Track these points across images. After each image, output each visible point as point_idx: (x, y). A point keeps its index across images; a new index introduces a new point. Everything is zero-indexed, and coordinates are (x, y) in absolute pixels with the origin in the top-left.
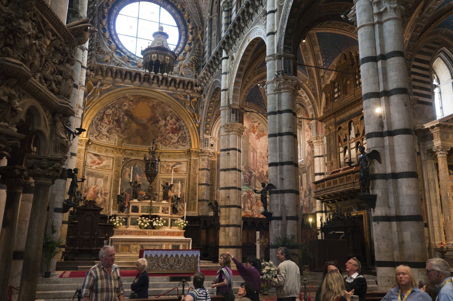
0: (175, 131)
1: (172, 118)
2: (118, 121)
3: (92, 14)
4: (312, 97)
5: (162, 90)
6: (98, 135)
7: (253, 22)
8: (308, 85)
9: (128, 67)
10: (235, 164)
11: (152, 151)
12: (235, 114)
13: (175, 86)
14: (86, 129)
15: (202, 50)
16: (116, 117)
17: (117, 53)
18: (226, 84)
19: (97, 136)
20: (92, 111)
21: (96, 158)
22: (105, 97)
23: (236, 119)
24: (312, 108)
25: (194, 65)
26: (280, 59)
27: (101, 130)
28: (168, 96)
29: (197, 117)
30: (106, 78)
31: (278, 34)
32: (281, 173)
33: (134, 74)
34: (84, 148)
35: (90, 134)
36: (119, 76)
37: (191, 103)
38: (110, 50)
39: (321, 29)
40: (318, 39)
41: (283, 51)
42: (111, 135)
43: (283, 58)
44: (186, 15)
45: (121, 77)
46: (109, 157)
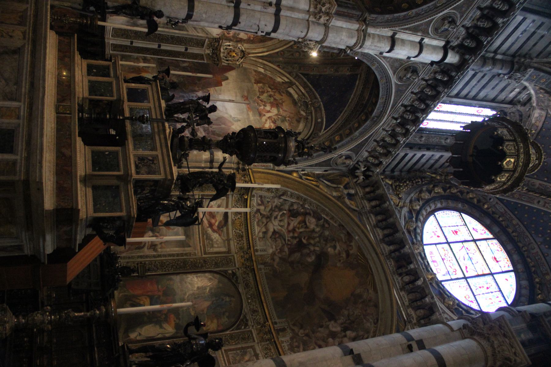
2: (300, 246)
16: (307, 240)
17: (410, 212)
19: (261, 214)
21: (220, 218)
22: (335, 203)
27: (273, 218)
30: (365, 201)
38: (408, 201)
42: (270, 240)
46: (229, 245)
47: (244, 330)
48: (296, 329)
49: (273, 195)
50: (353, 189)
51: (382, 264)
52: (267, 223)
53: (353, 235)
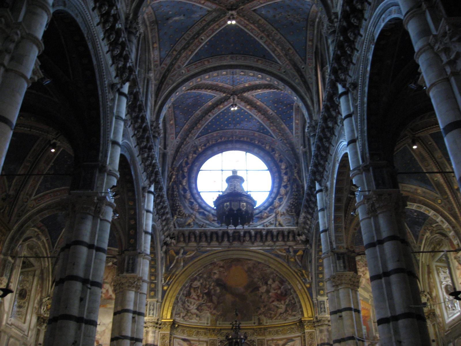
0: (280, 297)
1: (274, 281)
2: (209, 294)
3: (152, 172)
4: (451, 220)
5: (257, 247)
6: (186, 315)
7: (337, 137)
8: (441, 205)
9: (214, 227)
10: (351, 330)
11: (236, 326)
12: (341, 261)
13: (272, 239)
14: (15, 290)
15: (301, 190)
16: (206, 289)
17: (200, 213)
18: (325, 223)
19: (185, 316)
20: (175, 286)
22: (189, 267)
23: (345, 267)
24: (454, 234)
25: (293, 210)
26: (369, 170)
28: (266, 253)
29: (306, 274)
31: (359, 140)
32: (396, 332)
33: (220, 233)
34: (169, 332)
35: (176, 314)
36: (204, 239)
37: (296, 257)
39: (433, 128)
40: (436, 142)
41: (370, 159)
42: (202, 313)
43: (371, 169)
44: (277, 155)
45: (206, 240)
47: (257, 342)
48: (260, 312)
49: (176, 306)
50: (180, 250)
51: (235, 250)
52: (191, 313)
53: (213, 262)
